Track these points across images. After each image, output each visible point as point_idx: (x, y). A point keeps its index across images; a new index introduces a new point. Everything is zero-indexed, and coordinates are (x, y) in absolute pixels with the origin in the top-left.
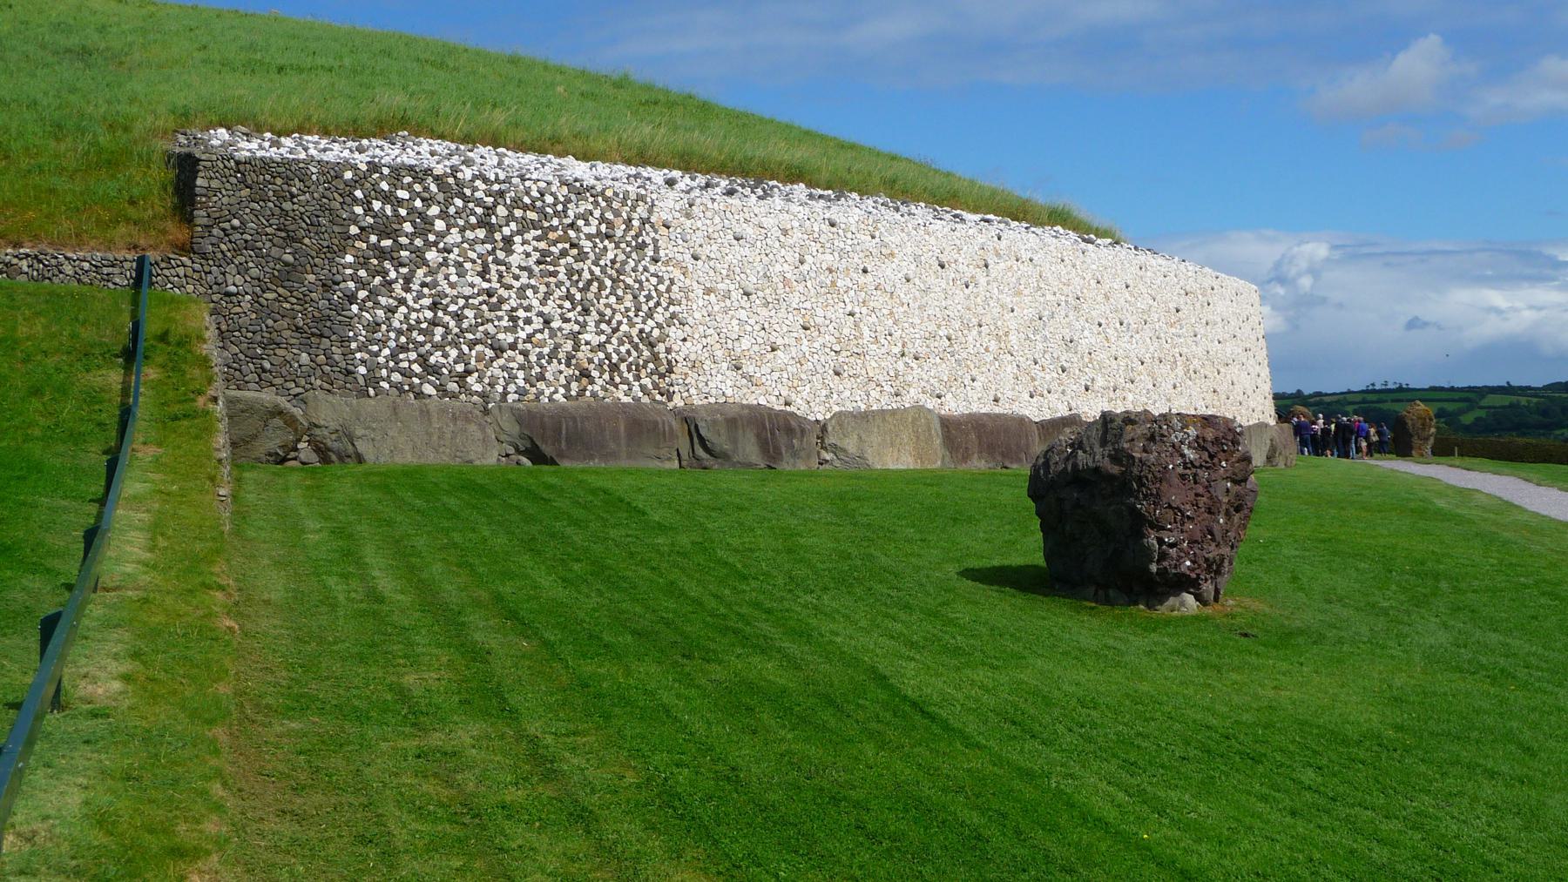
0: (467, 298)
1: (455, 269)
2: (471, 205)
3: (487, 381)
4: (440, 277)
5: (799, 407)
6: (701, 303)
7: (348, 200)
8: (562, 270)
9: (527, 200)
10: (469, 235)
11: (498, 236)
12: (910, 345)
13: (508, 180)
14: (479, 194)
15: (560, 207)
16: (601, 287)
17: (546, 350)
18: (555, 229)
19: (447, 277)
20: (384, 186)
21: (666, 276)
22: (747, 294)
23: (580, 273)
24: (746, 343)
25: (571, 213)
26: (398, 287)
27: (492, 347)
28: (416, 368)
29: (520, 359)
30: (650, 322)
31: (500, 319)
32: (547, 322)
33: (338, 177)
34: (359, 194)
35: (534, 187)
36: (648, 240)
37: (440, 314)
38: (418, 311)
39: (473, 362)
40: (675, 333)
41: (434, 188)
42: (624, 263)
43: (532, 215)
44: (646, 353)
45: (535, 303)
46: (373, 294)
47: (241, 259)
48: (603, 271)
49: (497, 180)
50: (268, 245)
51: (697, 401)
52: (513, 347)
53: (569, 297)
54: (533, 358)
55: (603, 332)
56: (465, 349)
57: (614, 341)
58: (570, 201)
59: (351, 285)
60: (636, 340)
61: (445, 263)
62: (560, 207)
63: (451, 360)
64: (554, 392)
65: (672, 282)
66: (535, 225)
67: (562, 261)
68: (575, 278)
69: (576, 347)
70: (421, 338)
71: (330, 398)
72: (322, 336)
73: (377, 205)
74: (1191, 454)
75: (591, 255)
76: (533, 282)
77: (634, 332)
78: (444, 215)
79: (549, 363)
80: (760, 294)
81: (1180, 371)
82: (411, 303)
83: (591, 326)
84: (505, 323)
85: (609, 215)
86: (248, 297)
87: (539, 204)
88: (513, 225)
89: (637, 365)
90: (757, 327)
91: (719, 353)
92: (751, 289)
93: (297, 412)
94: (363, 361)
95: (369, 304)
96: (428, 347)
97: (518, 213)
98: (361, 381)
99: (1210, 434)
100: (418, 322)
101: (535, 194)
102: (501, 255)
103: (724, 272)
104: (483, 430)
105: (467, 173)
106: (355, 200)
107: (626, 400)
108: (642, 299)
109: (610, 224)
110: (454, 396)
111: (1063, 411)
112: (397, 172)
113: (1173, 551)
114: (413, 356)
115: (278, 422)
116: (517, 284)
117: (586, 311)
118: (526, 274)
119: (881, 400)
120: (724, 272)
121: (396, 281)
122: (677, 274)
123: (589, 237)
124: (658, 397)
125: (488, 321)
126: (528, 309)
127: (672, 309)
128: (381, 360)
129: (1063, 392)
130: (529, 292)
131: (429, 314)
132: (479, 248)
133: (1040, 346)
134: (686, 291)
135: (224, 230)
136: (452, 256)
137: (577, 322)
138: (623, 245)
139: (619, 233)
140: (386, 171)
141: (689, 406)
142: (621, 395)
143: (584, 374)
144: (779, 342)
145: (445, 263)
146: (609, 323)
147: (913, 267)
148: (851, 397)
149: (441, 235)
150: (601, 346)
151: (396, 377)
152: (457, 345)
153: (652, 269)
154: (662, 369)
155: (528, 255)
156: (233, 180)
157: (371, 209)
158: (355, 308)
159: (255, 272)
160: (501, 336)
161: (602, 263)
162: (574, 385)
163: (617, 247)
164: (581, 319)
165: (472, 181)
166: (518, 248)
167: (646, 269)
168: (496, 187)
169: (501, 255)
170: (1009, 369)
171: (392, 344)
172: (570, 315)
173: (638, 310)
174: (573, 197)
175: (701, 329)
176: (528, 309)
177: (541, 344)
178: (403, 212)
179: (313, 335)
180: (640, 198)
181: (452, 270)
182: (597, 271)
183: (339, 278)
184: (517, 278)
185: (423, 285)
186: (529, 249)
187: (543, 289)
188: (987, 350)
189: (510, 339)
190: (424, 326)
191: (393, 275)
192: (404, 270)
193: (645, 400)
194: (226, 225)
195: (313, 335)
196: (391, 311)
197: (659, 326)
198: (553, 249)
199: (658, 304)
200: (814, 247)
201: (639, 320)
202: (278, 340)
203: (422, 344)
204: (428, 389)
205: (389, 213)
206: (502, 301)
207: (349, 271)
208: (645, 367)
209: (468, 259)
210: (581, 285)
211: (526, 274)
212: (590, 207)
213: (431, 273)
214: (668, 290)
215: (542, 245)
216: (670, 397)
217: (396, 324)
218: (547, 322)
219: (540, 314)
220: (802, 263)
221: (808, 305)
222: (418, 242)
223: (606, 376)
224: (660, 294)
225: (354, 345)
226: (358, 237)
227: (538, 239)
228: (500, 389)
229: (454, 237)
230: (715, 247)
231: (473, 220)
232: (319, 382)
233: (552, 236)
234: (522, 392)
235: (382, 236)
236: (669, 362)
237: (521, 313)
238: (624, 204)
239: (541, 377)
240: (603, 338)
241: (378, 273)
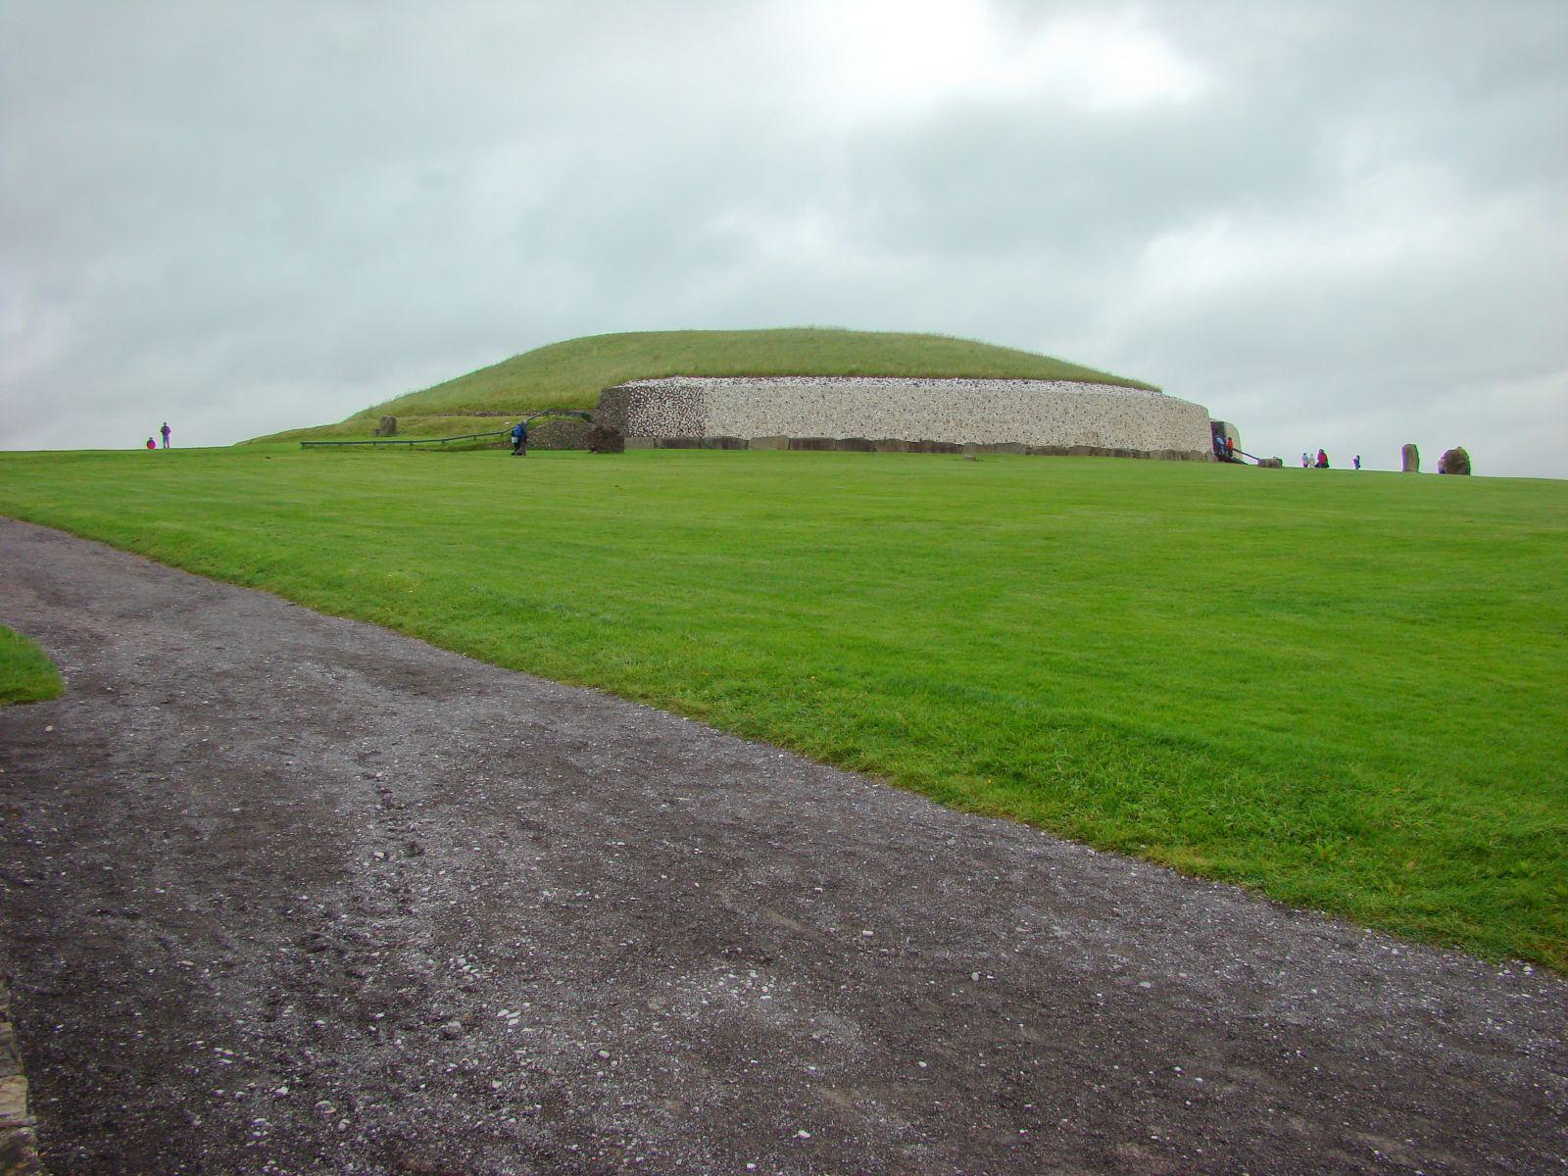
1: (652, 407)
5: (744, 436)
32: (673, 419)
64: (673, 435)
218: (673, 419)
235: (637, 402)
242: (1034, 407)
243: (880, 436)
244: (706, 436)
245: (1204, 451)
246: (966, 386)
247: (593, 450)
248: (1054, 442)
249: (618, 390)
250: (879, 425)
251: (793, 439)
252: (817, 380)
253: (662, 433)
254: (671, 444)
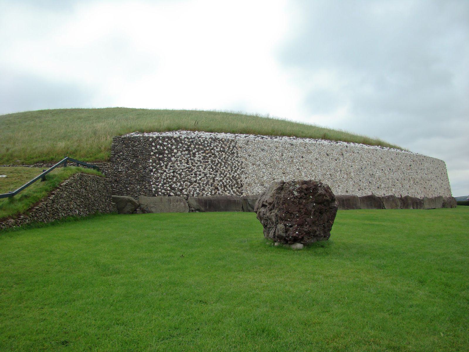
0: (183, 169)
2: (184, 145)
3: (188, 191)
4: (175, 164)
6: (251, 168)
7: (151, 146)
8: (210, 161)
9: (199, 143)
10: (183, 153)
11: (191, 153)
12: (317, 177)
13: (194, 138)
14: (186, 142)
15: (209, 144)
16: (221, 165)
17: (205, 182)
18: (208, 150)
19: (177, 164)
20: (160, 142)
21: (240, 161)
22: (266, 165)
23: (215, 161)
24: (265, 178)
25: (212, 146)
26: (164, 167)
27: (190, 182)
28: (169, 188)
29: (198, 185)
30: (236, 174)
31: (192, 174)
32: (205, 175)
33: (148, 140)
34: (153, 144)
35: (202, 139)
36: (235, 152)
37: (175, 174)
38: (169, 173)
39: (184, 186)
40: (243, 176)
41: (174, 141)
42: (228, 158)
43: (201, 147)
44: (235, 182)
45: (202, 170)
46: (157, 170)
47: (123, 162)
48: (222, 160)
49: (191, 138)
50: (129, 158)
51: (250, 194)
52: (196, 182)
53: (212, 168)
54: (201, 185)
55: (222, 177)
56: (182, 183)
57: (225, 179)
58: (212, 142)
59: (151, 167)
60: (231, 178)
61: (177, 160)
62: (209, 144)
63: (178, 186)
64: (208, 193)
65: (242, 162)
66: (202, 149)
67: (210, 158)
68: (213, 163)
69: (214, 181)
70: (170, 180)
71: (145, 197)
72: (143, 181)
73: (158, 147)
74: (296, 193)
75: (218, 157)
76: (201, 164)
77: (231, 176)
78: (176, 148)
79: (206, 186)
80: (269, 165)
81: (412, 182)
82: (167, 171)
83: (218, 175)
84: (193, 176)
85: (223, 146)
86: (124, 172)
87: (203, 144)
88: (196, 150)
89: (232, 185)
90: (268, 174)
91: (257, 181)
92: (266, 163)
93: (136, 201)
94: (154, 187)
95: (156, 172)
96: (172, 183)
97: (197, 146)
98: (154, 192)
99: (305, 186)
100: (169, 176)
101: (202, 141)
102: (192, 158)
103: (258, 159)
104: (185, 204)
105: (183, 137)
106: (153, 146)
107: (228, 195)
108: (233, 167)
109: (223, 148)
110: (179, 195)
111: (370, 194)
112: (164, 138)
113: (291, 229)
114: (168, 185)
115: (129, 204)
116: (197, 165)
117: (217, 172)
118: (199, 162)
120: (258, 159)
121: (163, 166)
122: (244, 160)
123: (217, 152)
124: (238, 194)
125: (188, 175)
126: (200, 171)
127: (242, 170)
128: (159, 187)
129: (370, 189)
130: (200, 167)
131: (172, 174)
132: (186, 156)
133: (362, 176)
134: (247, 165)
135: (118, 155)
136: (179, 159)
137: (214, 174)
138: (227, 153)
139: (226, 150)
140: (161, 138)
141: (248, 196)
142: (227, 194)
143: (217, 188)
144: (275, 177)
145: (177, 160)
146: (223, 174)
147: (318, 156)
149: (176, 153)
150: (221, 181)
151: (163, 191)
152: (180, 182)
153: (236, 159)
154: (239, 186)
155: (200, 157)
156: (121, 143)
157: (157, 148)
158: (152, 173)
159: (126, 166)
160: (192, 179)
161: (221, 158)
162: (213, 192)
163: (226, 154)
164: (215, 173)
165: (184, 139)
166: (197, 156)
167: (234, 159)
168: (191, 140)
169: (192, 158)
170: (351, 183)
171: (162, 182)
172: (212, 173)
173: (232, 171)
174: (213, 141)
175: (251, 175)
176: (200, 171)
177: (204, 181)
178: (165, 148)
179: (141, 181)
180: (233, 140)
181: (179, 162)
182: (220, 160)
183: (147, 166)
184: (197, 163)
185: (171, 166)
186: (200, 156)
187: (204, 166)
188: (343, 178)
189: (195, 180)
190: (171, 177)
191: (162, 164)
192: (165, 163)
193: (234, 195)
194: (119, 154)
195: (141, 181)
196: (162, 174)
197: (238, 174)
198: (207, 155)
199: (238, 169)
200: (286, 151)
201: (232, 173)
202: (132, 182)
203: (170, 182)
204: (172, 194)
205: (162, 148)
206: (193, 170)
207: (150, 164)
208: (234, 186)
209: (183, 159)
210: (215, 164)
211: (199, 162)
212: (218, 144)
213: (173, 163)
214: (241, 165)
215: (204, 154)
216: (242, 194)
217: (163, 177)
218: (205, 175)
219: (203, 173)
220: (282, 155)
221: (284, 167)
222: (169, 156)
223: (223, 189)
224: (239, 166)
225: (152, 183)
226: (153, 155)
227: (202, 153)
228: (192, 193)
229: (179, 154)
230: (255, 153)
231: (184, 149)
232: (142, 193)
233: (207, 152)
234: (198, 194)
235: (160, 154)
236: (241, 184)
237: (198, 173)
238: (228, 142)
239: (204, 190)
240: (222, 178)
241: (158, 164)
244: (244, 195)
247: (286, 241)
250: (379, 183)
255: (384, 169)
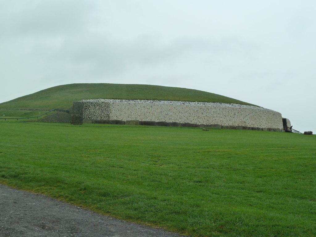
5: (123, 120)
64: (99, 119)
111: (164, 121)
112: (88, 102)
119: (133, 119)
134: (112, 110)
148: (129, 119)
242: (224, 112)
243: (171, 121)
245: (281, 129)
246: (201, 104)
248: (231, 124)
249: (80, 103)
251: (140, 122)
252: (149, 101)
253: (94, 118)
254: (97, 122)
255: (175, 112)
